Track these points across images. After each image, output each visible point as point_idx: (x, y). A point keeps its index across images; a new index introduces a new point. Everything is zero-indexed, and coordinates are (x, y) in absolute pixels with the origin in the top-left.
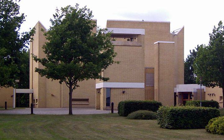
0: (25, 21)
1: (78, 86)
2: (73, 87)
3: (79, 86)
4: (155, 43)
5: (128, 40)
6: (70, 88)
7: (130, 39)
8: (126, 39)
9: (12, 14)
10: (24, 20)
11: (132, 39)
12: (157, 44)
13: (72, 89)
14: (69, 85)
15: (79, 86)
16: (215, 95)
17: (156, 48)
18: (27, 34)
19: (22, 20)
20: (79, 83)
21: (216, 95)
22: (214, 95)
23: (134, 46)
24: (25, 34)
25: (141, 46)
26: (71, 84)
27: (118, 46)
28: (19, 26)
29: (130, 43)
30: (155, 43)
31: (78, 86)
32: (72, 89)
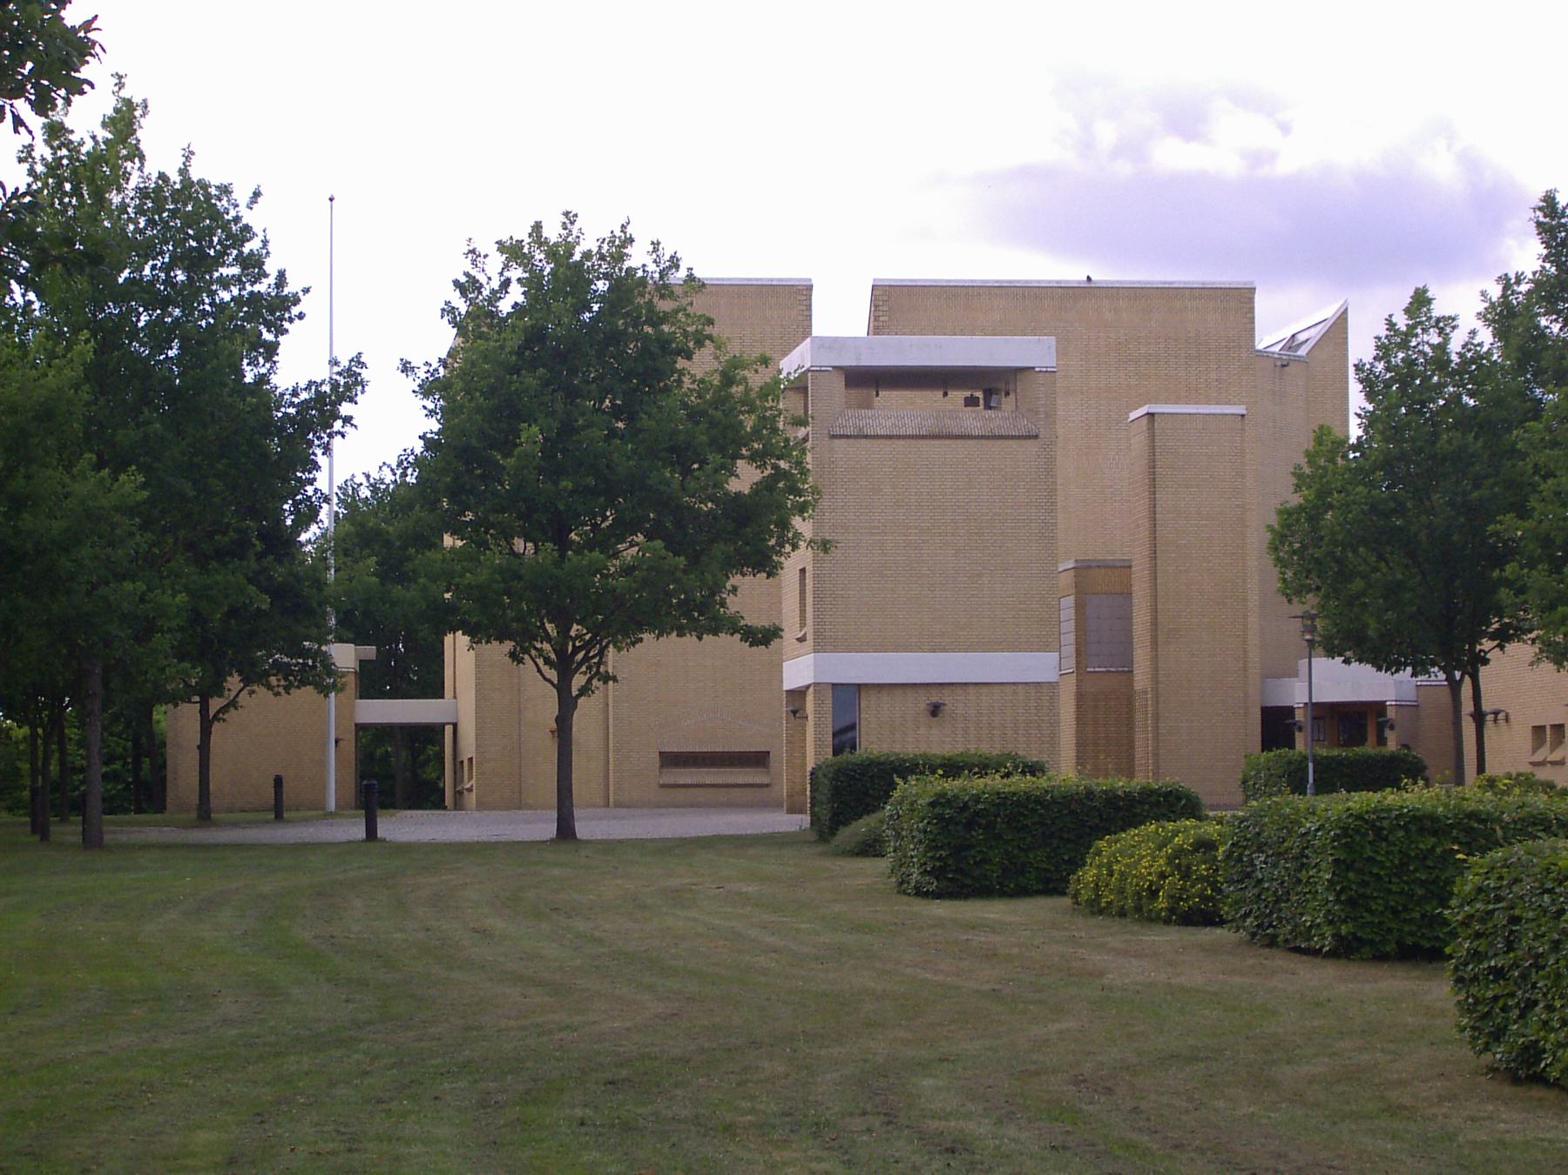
0: (301, 316)
1: (606, 678)
2: (578, 681)
3: (615, 679)
4: (1133, 415)
5: (971, 402)
6: (563, 687)
7: (979, 394)
8: (958, 396)
9: (225, 283)
10: (295, 311)
11: (994, 397)
12: (1145, 421)
13: (575, 693)
14: (552, 674)
15: (615, 679)
16: (1507, 719)
17: (1139, 441)
18: (316, 390)
19: (287, 316)
20: (613, 659)
21: (1512, 717)
22: (1501, 716)
23: (995, 437)
24: (304, 396)
25: (1036, 437)
26: (565, 667)
27: (899, 437)
28: (271, 350)
29: (974, 419)
30: (1133, 415)
31: (606, 678)
32: (575, 693)
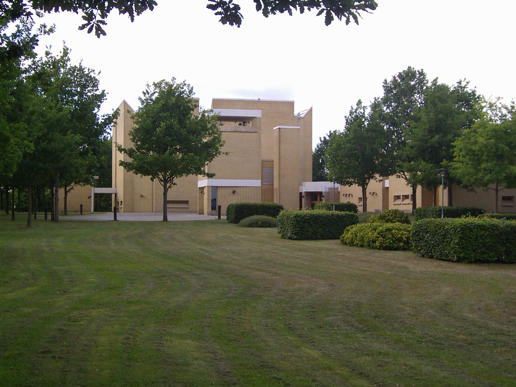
0: (106, 99)
1: (174, 184)
2: (168, 185)
3: (176, 184)
4: (274, 128)
5: (240, 124)
6: (165, 186)
7: (242, 123)
8: (238, 123)
9: (89, 91)
10: (105, 98)
11: (245, 124)
12: (278, 130)
13: (167, 187)
14: (163, 183)
15: (176, 184)
16: (352, 196)
17: (276, 134)
18: (109, 116)
19: (103, 99)
20: (175, 180)
21: (353, 195)
22: (351, 195)
23: (248, 132)
24: (106, 117)
25: (257, 132)
26: (165, 181)
27: (227, 132)
28: (99, 106)
29: (242, 128)
30: (274, 128)
31: (174, 184)
32: (167, 187)
